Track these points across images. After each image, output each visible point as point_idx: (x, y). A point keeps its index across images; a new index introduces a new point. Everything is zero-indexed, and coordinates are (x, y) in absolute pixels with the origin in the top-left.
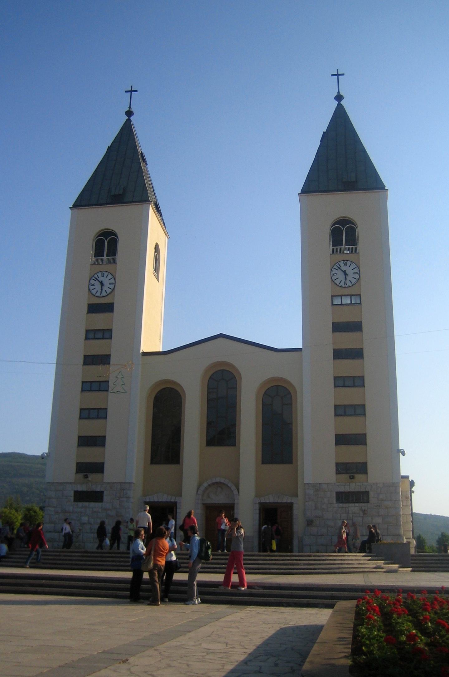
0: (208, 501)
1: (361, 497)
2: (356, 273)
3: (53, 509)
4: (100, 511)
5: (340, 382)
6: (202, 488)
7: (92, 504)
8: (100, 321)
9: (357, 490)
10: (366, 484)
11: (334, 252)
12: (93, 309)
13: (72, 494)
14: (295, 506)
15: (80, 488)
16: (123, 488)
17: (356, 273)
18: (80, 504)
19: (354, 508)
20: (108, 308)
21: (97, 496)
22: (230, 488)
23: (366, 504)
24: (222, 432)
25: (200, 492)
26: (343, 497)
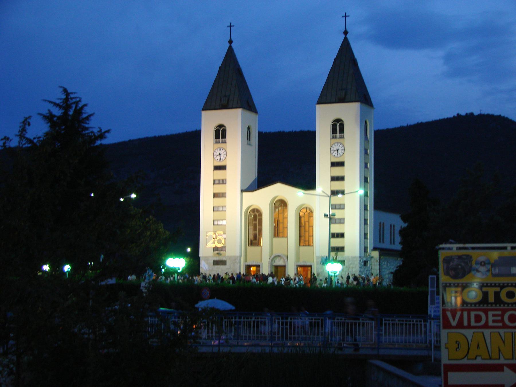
0: (275, 264)
11: (334, 138)
12: (217, 168)
16: (235, 259)
20: (223, 168)
25: (271, 260)
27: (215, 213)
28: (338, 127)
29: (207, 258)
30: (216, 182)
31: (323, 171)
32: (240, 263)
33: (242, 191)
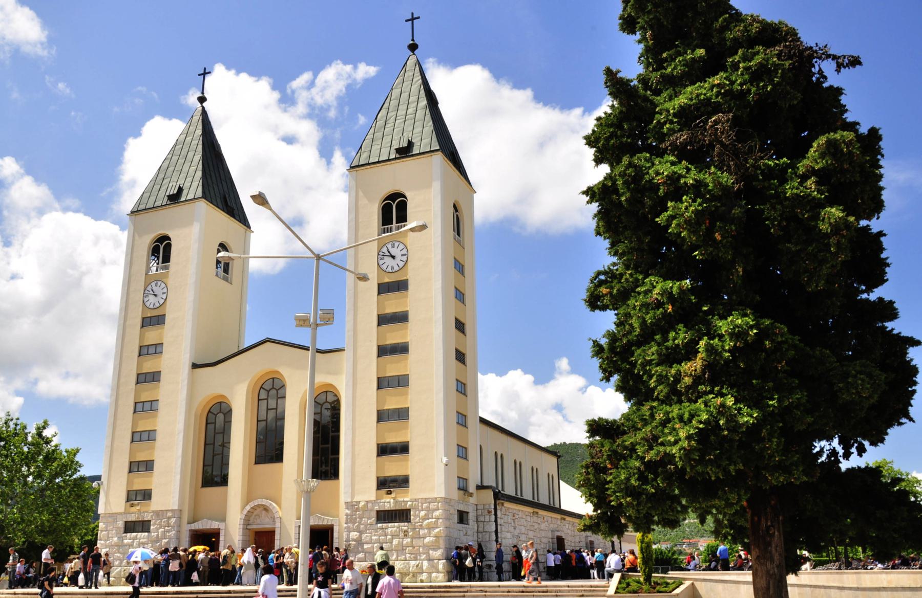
1: (401, 515)
8: (152, 336)
9: (398, 508)
13: (121, 524)
14: (336, 529)
18: (129, 534)
19: (392, 527)
24: (269, 449)
26: (386, 516)
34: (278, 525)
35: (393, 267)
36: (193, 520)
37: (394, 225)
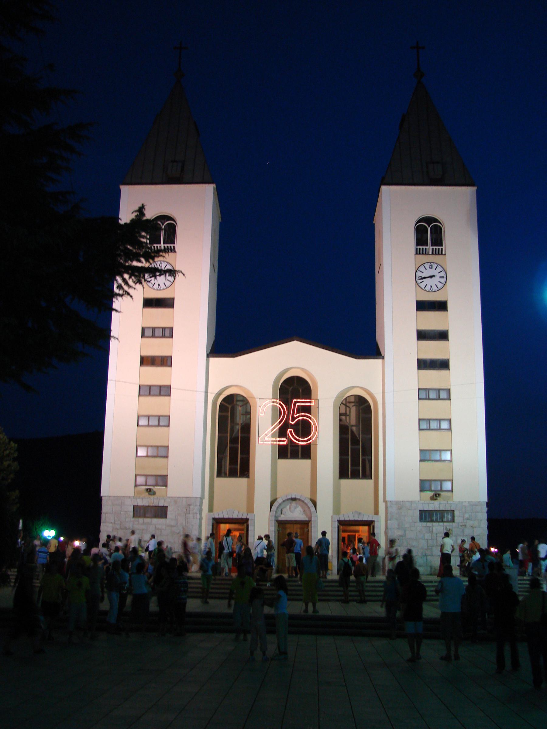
0: (282, 518)
2: (443, 277)
3: (111, 525)
4: (164, 527)
5: (425, 394)
6: (276, 504)
7: (155, 521)
9: (441, 508)
10: (451, 502)
11: (418, 252)
13: (131, 509)
15: (140, 503)
17: (443, 277)
18: (141, 520)
21: (161, 512)
22: (307, 505)
23: (451, 524)
26: (426, 516)
27: (142, 398)
28: (429, 234)
29: (119, 500)
30: (148, 333)
31: (396, 318)
32: (201, 514)
33: (208, 356)
34: (313, 519)
35: (431, 287)
36: (211, 510)
37: (429, 247)
